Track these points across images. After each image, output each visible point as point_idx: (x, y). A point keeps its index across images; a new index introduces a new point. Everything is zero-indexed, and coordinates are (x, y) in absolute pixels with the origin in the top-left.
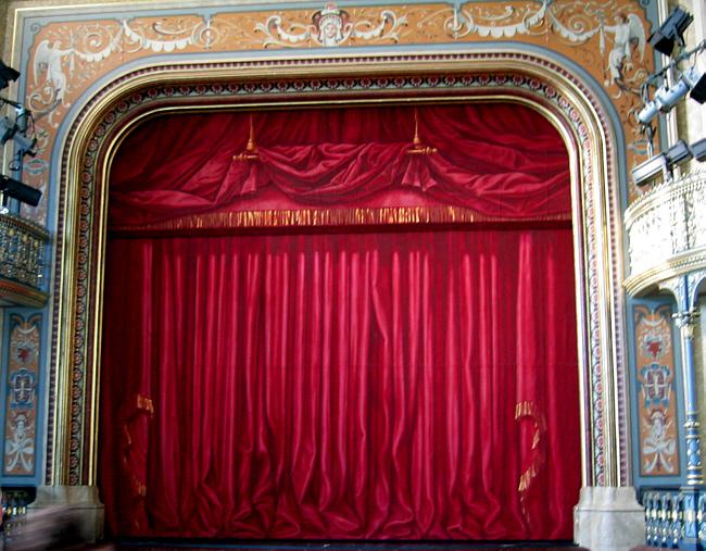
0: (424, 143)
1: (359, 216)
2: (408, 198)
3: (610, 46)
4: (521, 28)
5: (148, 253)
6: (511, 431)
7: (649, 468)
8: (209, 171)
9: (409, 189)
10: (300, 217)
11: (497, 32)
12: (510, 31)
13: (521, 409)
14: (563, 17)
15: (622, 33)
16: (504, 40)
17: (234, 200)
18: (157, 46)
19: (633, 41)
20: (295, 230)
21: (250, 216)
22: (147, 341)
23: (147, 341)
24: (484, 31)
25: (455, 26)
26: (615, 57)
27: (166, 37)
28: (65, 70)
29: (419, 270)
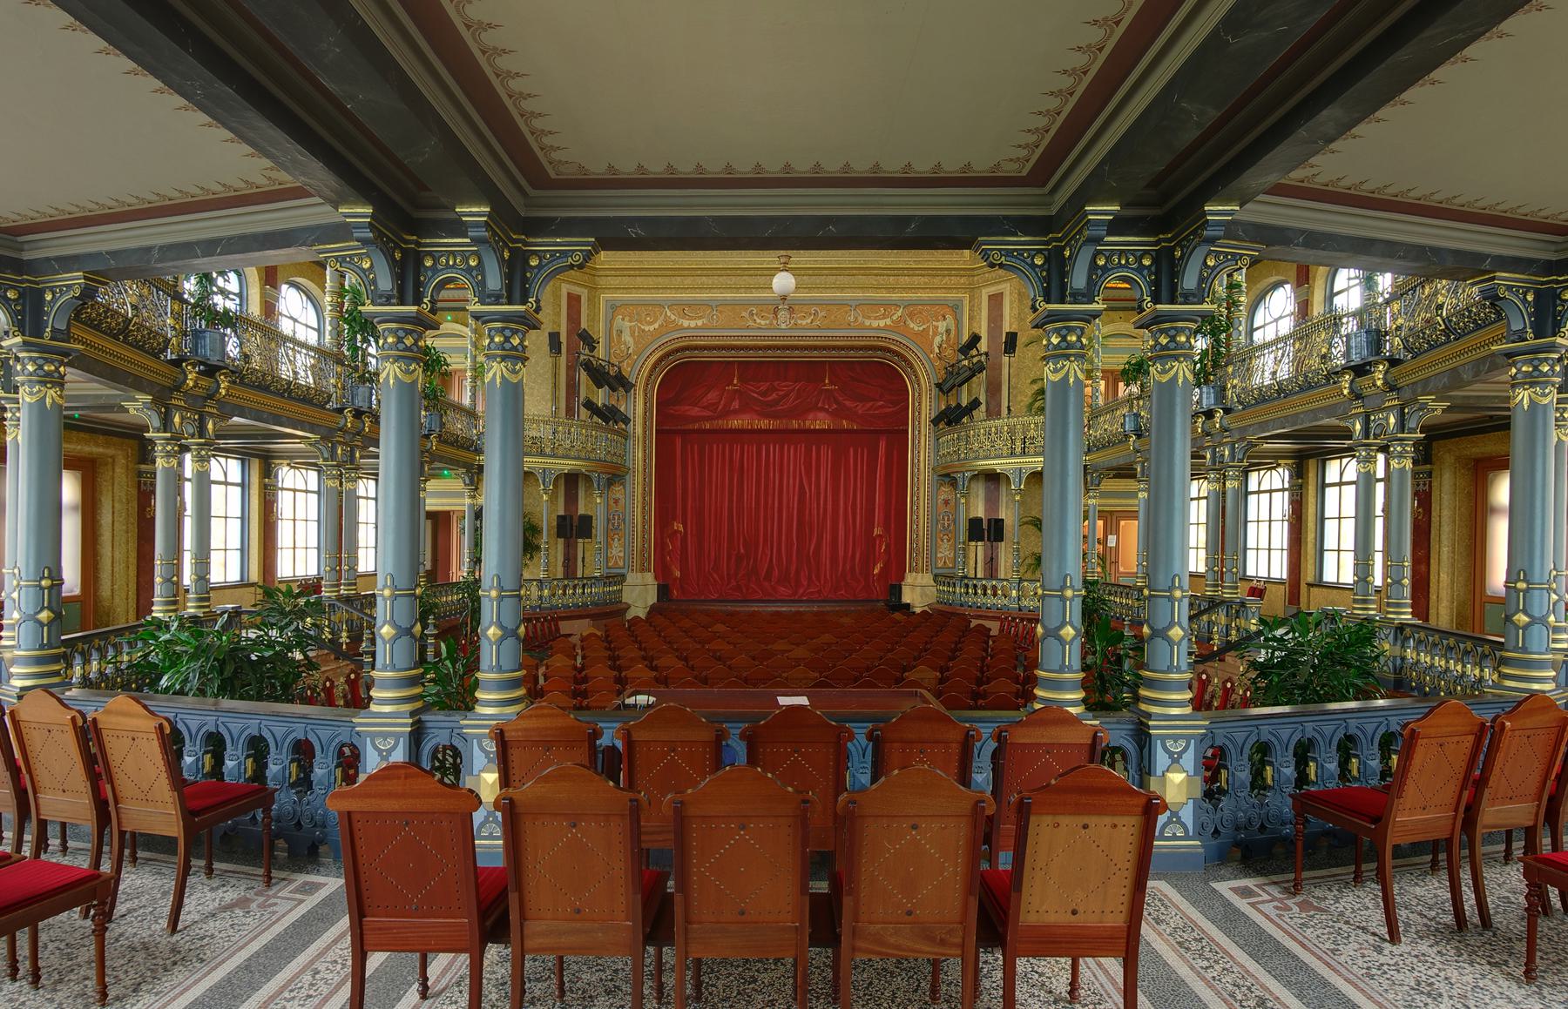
0: (831, 383)
1: (795, 424)
2: (821, 415)
3: (935, 334)
4: (888, 322)
5: (679, 442)
6: (871, 542)
7: (940, 564)
8: (712, 396)
9: (822, 409)
10: (764, 424)
11: (875, 324)
12: (882, 323)
13: (877, 531)
14: (911, 316)
15: (942, 326)
16: (878, 328)
17: (727, 413)
18: (686, 323)
19: (948, 331)
20: (760, 431)
21: (736, 423)
22: (679, 492)
23: (679, 492)
24: (867, 323)
25: (852, 319)
26: (938, 340)
27: (691, 318)
28: (632, 335)
29: (826, 454)
